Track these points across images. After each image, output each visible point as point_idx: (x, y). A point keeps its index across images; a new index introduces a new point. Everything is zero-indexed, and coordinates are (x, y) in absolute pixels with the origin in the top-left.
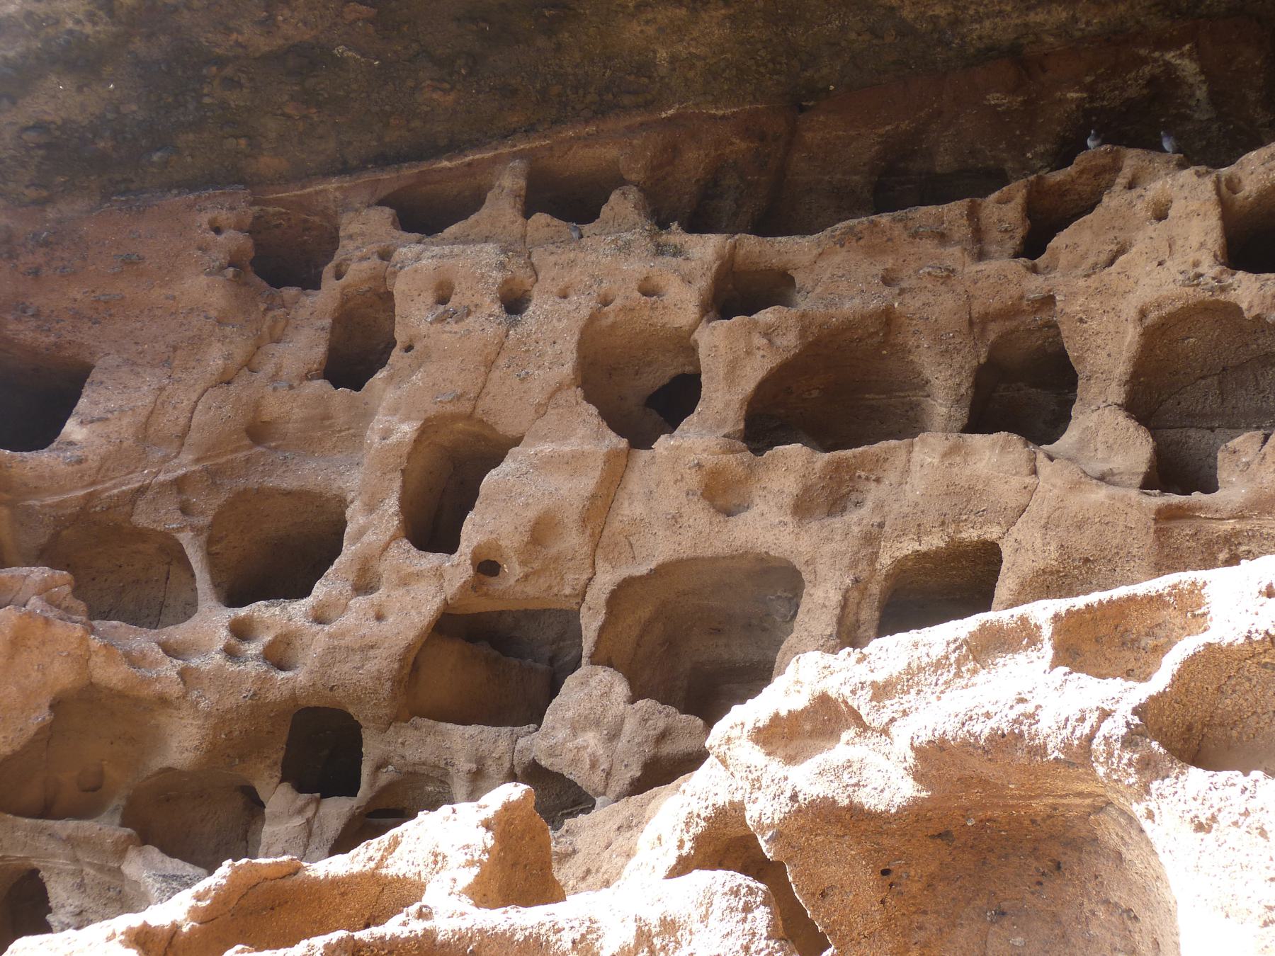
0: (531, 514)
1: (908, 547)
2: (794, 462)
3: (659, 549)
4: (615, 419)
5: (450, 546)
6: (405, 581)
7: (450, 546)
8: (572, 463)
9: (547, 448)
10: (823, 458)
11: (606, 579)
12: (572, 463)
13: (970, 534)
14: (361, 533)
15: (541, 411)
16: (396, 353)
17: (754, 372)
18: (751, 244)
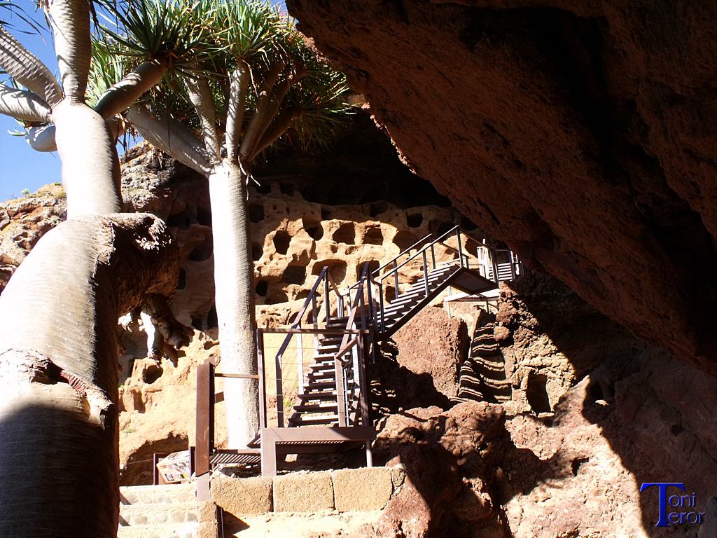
0: (302, 250)
1: (365, 260)
2: (343, 247)
3: (321, 259)
4: (311, 235)
5: (285, 253)
6: (280, 259)
7: (285, 253)
8: (307, 242)
9: (301, 239)
10: (349, 246)
11: (313, 262)
12: (307, 242)
13: (374, 260)
14: (268, 251)
15: (297, 232)
16: (265, 217)
17: (334, 230)
18: (325, 206)
